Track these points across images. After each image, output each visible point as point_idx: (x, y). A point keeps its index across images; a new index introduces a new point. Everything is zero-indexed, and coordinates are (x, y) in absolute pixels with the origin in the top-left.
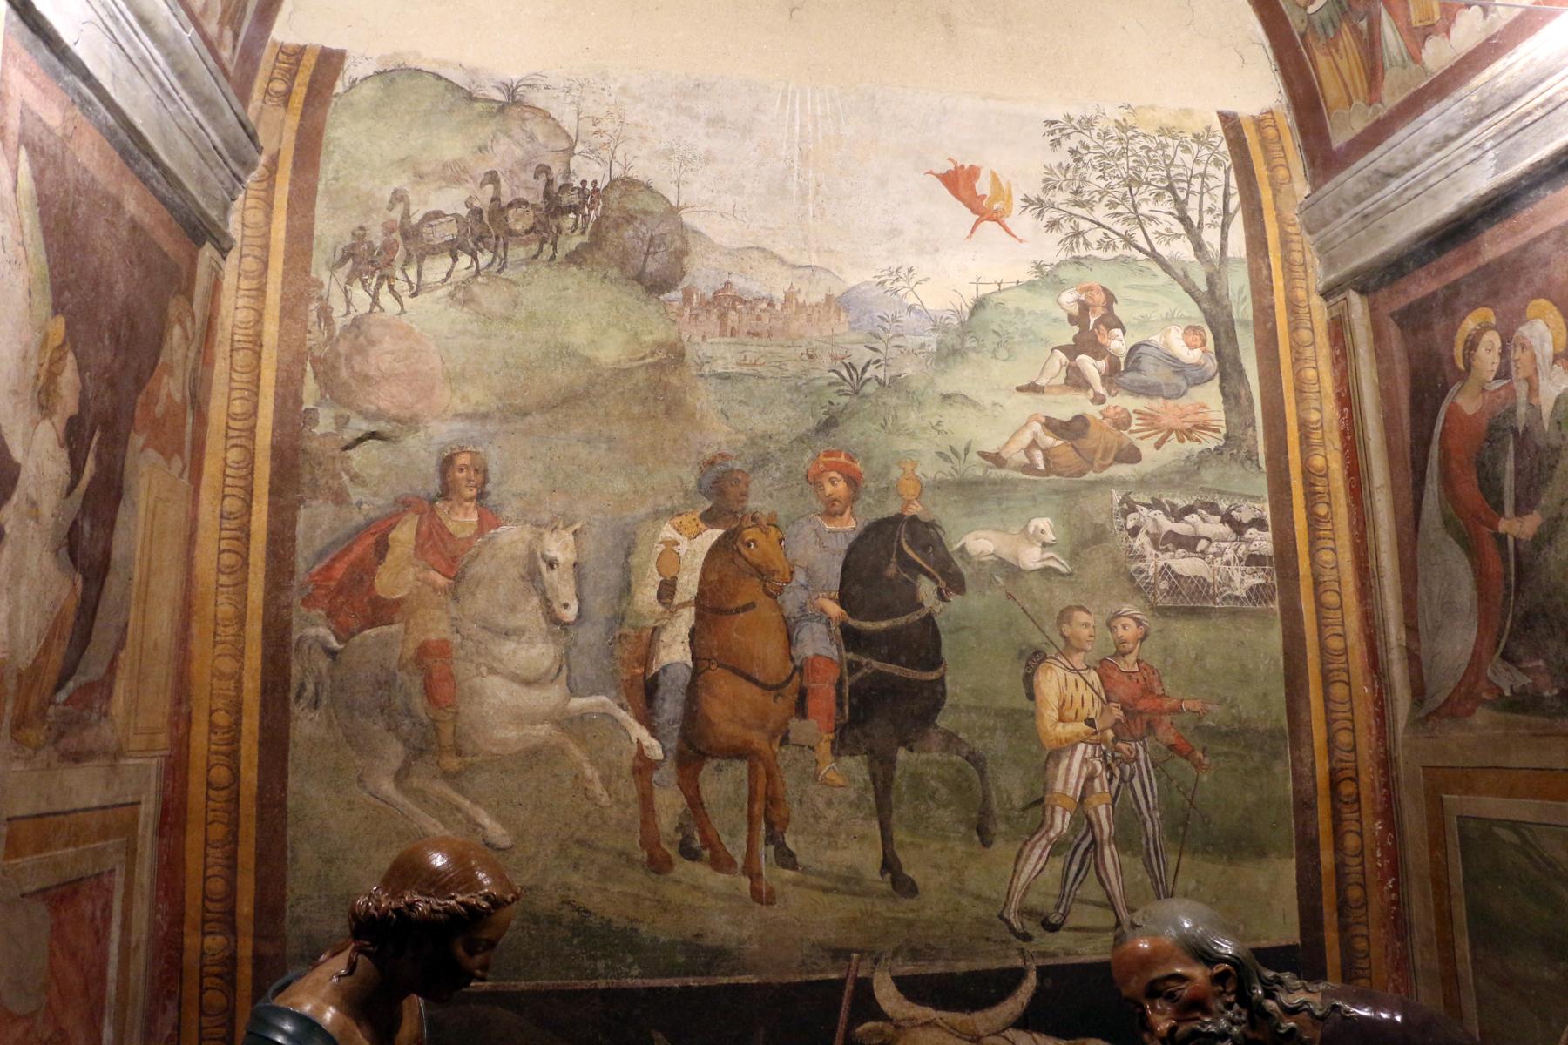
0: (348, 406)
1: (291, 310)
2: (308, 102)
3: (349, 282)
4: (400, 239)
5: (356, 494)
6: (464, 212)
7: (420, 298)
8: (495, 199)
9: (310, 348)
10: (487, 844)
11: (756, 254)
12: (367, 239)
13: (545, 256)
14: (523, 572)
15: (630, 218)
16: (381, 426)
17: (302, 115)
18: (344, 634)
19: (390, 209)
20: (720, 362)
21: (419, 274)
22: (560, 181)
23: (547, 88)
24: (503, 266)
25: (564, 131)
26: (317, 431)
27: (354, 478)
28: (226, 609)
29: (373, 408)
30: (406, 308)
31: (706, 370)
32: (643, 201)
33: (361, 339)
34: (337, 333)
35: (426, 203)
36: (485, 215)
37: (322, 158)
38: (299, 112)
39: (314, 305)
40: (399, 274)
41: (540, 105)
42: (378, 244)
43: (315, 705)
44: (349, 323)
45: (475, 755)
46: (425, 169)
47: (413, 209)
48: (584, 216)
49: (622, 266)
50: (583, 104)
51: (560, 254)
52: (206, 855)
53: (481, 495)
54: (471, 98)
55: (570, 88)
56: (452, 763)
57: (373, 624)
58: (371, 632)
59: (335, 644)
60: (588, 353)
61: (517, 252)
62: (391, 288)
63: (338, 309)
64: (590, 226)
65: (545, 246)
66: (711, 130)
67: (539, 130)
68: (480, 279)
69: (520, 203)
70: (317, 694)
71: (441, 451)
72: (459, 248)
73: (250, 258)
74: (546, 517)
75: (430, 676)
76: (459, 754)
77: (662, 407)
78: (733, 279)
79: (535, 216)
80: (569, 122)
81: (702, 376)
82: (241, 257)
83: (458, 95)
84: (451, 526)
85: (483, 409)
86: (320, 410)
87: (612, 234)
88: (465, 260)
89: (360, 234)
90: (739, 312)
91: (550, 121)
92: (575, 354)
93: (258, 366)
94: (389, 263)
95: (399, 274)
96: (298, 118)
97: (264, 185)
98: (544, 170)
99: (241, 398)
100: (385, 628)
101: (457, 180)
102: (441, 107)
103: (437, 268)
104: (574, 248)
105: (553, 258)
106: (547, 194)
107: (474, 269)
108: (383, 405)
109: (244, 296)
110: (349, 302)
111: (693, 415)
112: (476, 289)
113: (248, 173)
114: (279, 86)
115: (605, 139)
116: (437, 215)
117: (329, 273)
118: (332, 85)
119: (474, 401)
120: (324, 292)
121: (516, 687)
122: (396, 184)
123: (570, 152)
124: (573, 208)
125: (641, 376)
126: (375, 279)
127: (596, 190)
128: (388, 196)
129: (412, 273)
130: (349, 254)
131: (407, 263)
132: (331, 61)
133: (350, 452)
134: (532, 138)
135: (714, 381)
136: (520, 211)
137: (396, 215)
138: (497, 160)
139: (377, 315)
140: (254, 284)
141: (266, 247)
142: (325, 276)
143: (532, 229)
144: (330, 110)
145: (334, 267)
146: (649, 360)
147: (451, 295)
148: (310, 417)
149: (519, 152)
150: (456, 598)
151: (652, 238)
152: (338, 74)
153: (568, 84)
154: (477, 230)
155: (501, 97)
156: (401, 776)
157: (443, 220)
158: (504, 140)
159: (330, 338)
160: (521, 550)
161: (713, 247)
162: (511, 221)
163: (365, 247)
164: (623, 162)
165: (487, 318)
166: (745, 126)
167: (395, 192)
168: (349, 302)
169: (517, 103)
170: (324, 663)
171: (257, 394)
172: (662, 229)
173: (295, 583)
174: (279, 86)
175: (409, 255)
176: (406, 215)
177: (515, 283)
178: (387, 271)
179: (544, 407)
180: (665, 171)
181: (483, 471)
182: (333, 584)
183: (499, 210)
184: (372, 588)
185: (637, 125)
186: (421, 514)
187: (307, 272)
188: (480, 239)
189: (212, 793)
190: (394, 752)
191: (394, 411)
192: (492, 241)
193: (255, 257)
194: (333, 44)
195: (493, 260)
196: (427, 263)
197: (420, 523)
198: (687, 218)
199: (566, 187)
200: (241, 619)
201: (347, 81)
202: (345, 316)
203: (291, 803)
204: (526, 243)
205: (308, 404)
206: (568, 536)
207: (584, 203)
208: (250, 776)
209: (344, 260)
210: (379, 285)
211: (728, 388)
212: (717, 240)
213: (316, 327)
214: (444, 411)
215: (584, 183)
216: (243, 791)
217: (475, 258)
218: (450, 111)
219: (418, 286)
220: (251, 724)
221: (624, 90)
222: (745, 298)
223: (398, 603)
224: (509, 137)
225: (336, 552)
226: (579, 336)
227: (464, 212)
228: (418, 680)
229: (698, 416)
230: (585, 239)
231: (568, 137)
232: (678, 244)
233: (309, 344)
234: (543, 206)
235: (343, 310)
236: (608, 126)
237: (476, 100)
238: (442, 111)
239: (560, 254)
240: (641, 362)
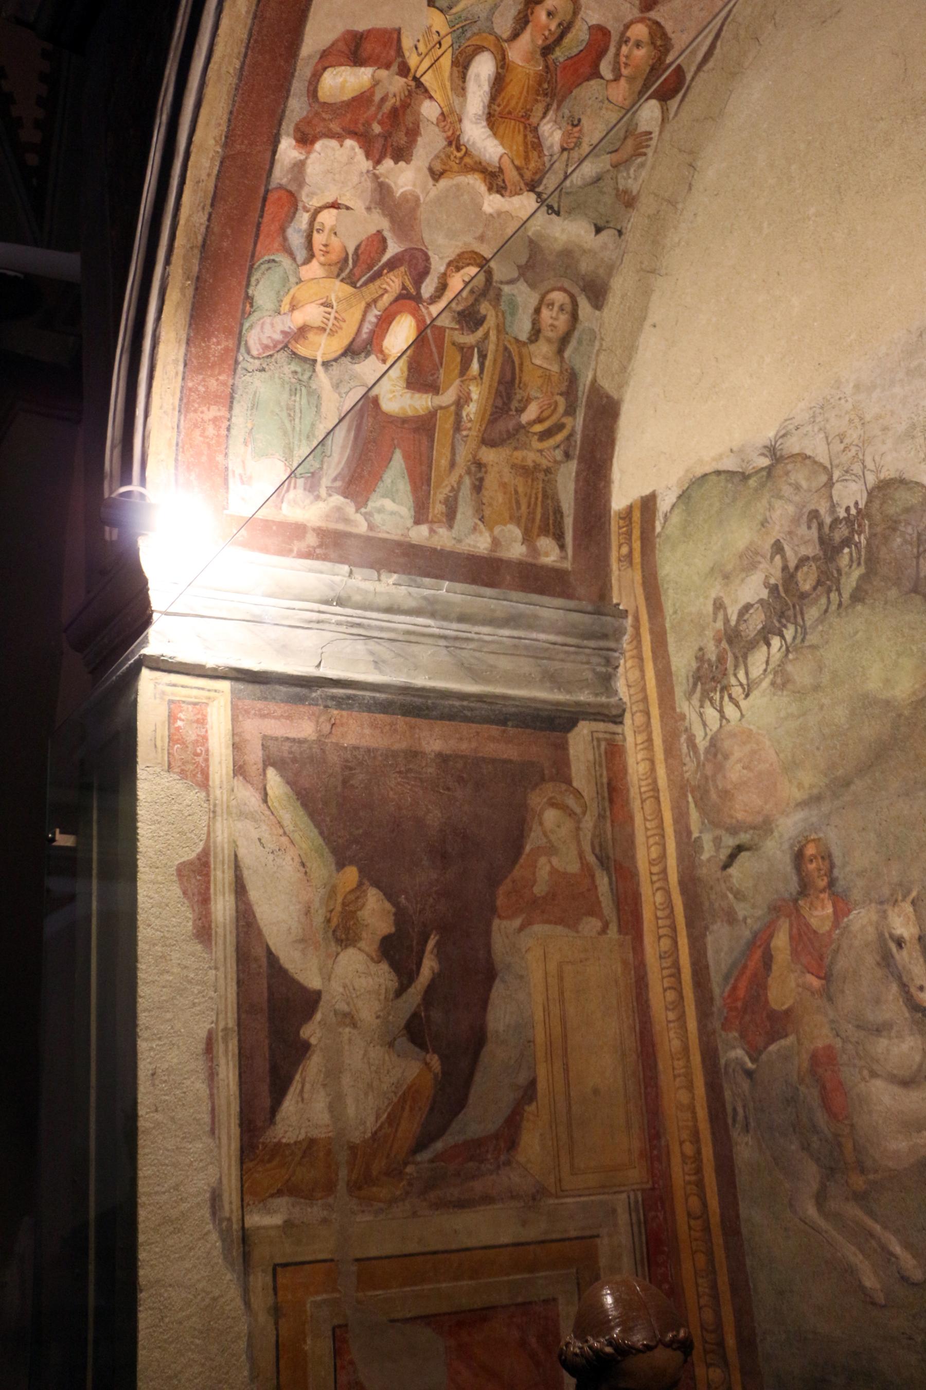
1: (670, 751)
2: (643, 553)
5: (742, 910)
8: (785, 568)
9: (688, 780)
10: (903, 1278)
12: (706, 657)
13: (834, 607)
14: (878, 959)
15: (893, 525)
16: (744, 837)
17: (642, 567)
18: (755, 1053)
19: (715, 621)
21: (747, 674)
22: (828, 520)
23: (797, 429)
24: (805, 633)
26: (705, 857)
27: (739, 896)
28: (676, 1044)
30: (744, 713)
32: (904, 498)
33: (719, 756)
34: (702, 758)
35: (736, 602)
36: (781, 588)
37: (663, 598)
39: (683, 738)
41: (796, 450)
42: (714, 658)
43: (746, 1128)
44: (707, 744)
45: (876, 1171)
46: (729, 567)
48: (856, 546)
49: (897, 583)
50: (828, 426)
51: (846, 595)
52: (697, 1285)
53: (832, 883)
54: (744, 477)
55: (814, 417)
56: (859, 1182)
57: (773, 1040)
58: (773, 1048)
59: (750, 1065)
60: (886, 695)
61: (812, 614)
63: (699, 732)
64: (863, 553)
67: (800, 476)
68: (791, 656)
69: (803, 560)
70: (746, 1118)
71: (791, 847)
72: (769, 633)
73: (638, 714)
74: (886, 891)
75: (824, 1087)
76: (863, 1171)
79: (818, 568)
80: (820, 452)
82: (633, 715)
83: (736, 479)
84: (814, 922)
85: (815, 791)
86: (703, 835)
87: (883, 553)
89: (700, 657)
91: (807, 462)
93: (660, 811)
94: (725, 674)
95: (733, 681)
98: (814, 515)
100: (783, 1042)
101: (752, 566)
102: (727, 500)
103: (758, 661)
104: (854, 584)
105: (840, 605)
106: (822, 540)
107: (784, 648)
108: (740, 816)
109: (642, 749)
110: (705, 725)
113: (618, 640)
116: (747, 607)
117: (687, 703)
118: (654, 528)
119: (807, 786)
120: (687, 723)
121: (896, 1089)
122: (713, 594)
126: (718, 693)
128: (710, 608)
129: (741, 675)
130: (698, 678)
131: (736, 667)
132: (648, 504)
133: (731, 870)
134: (797, 487)
136: (805, 569)
137: (719, 625)
139: (727, 728)
143: (819, 583)
145: (689, 695)
147: (773, 684)
148: (697, 846)
149: (791, 509)
150: (830, 999)
153: (811, 412)
155: (765, 462)
156: (821, 1198)
157: (751, 611)
158: (778, 504)
159: (698, 763)
160: (871, 934)
162: (801, 583)
163: (706, 666)
164: (873, 468)
165: (801, 694)
167: (715, 604)
168: (705, 725)
170: (745, 1085)
171: (663, 837)
173: (715, 1009)
174: (625, 550)
175: (736, 658)
176: (727, 621)
178: (725, 682)
179: (863, 769)
180: (913, 453)
181: (827, 857)
182: (739, 1004)
183: (789, 576)
184: (767, 1002)
185: (878, 417)
186: (789, 916)
187: (674, 709)
188: (782, 615)
189: (692, 1222)
190: (811, 1172)
193: (641, 711)
194: (647, 492)
195: (796, 631)
196: (750, 659)
197: (791, 925)
199: (836, 521)
200: (686, 1049)
201: (661, 518)
202: (704, 739)
203: (744, 1231)
206: (908, 908)
208: (714, 1202)
209: (695, 685)
210: (722, 698)
213: (688, 759)
214: (788, 804)
215: (848, 509)
216: (712, 1221)
217: (783, 637)
218: (734, 500)
219: (748, 685)
220: (708, 1152)
221: (857, 387)
223: (788, 1012)
225: (736, 973)
226: (873, 684)
228: (815, 1092)
230: (862, 570)
231: (825, 468)
234: (821, 554)
235: (702, 733)
236: (853, 436)
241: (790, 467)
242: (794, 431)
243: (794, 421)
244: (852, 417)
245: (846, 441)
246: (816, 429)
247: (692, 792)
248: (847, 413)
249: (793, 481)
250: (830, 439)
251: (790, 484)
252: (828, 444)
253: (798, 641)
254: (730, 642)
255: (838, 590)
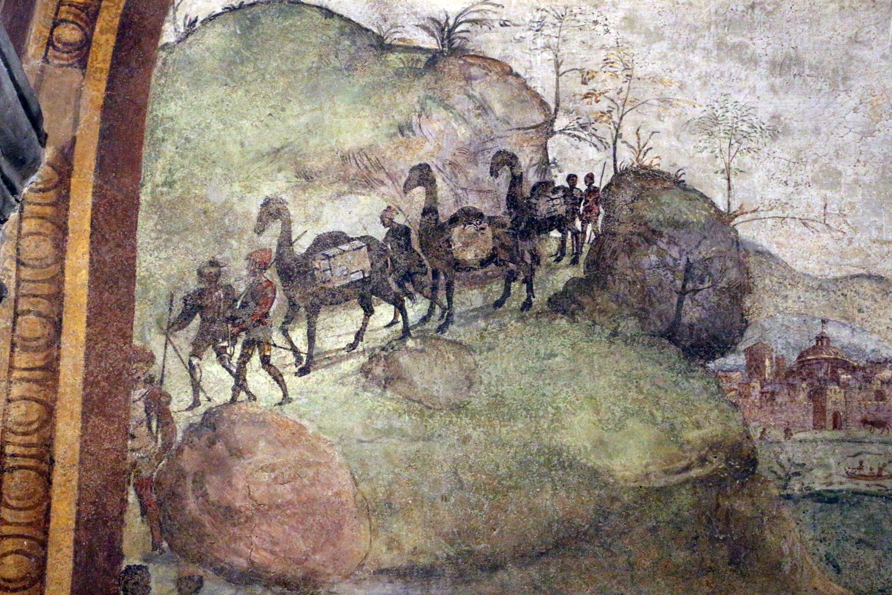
0: (200, 560)
2: (118, 60)
3: (196, 353)
4: (277, 280)
6: (379, 232)
7: (314, 376)
8: (429, 211)
9: (134, 465)
11: (867, 287)
12: (223, 281)
13: (514, 303)
15: (650, 235)
17: (111, 80)
19: (259, 231)
20: (819, 473)
21: (311, 338)
22: (532, 178)
23: (503, 25)
24: (448, 320)
25: (536, 95)
29: (241, 563)
30: (290, 394)
31: (795, 487)
33: (220, 446)
34: (179, 437)
35: (317, 220)
36: (414, 236)
37: (146, 151)
38: (104, 76)
40: (277, 338)
44: (198, 419)
46: (315, 164)
47: (296, 230)
48: (575, 234)
49: (642, 315)
50: (564, 49)
51: (540, 298)
55: (541, 23)
60: (595, 461)
62: (265, 361)
64: (586, 249)
65: (515, 286)
66: (778, 81)
68: (410, 343)
72: (372, 292)
73: (31, 317)
77: (724, 552)
78: (831, 331)
79: (495, 237)
81: (789, 497)
82: (16, 315)
85: (423, 561)
86: (151, 567)
87: (623, 263)
88: (384, 312)
90: (845, 386)
91: (511, 79)
92: (570, 465)
93: (47, 497)
94: (262, 320)
95: (277, 338)
96: (103, 85)
97: (52, 195)
98: (507, 160)
99: (17, 552)
101: (367, 182)
102: (336, 63)
104: (561, 286)
105: (527, 305)
106: (512, 200)
107: (400, 326)
108: (261, 557)
109: (22, 379)
110: (196, 387)
111: (778, 566)
112: (404, 360)
113: (25, 178)
114: (70, 34)
115: (604, 105)
116: (337, 239)
117: (163, 339)
118: (156, 32)
119: (408, 548)
120: (155, 370)
122: (267, 190)
123: (547, 129)
124: (559, 223)
125: (685, 499)
126: (239, 347)
127: (592, 191)
128: (255, 210)
129: (299, 336)
131: (289, 319)
134: (484, 108)
135: (811, 506)
136: (471, 229)
137: (270, 239)
138: (428, 147)
139: (245, 407)
140: (38, 359)
141: (57, 297)
142: (156, 343)
143: (492, 258)
144: (155, 71)
145: (172, 327)
146: (695, 473)
147: (365, 371)
149: (463, 132)
151: (689, 267)
152: (166, 13)
153: (538, 16)
154: (402, 262)
155: (431, 43)
157: (345, 247)
158: (439, 113)
159: (166, 446)
161: (792, 278)
162: (457, 245)
163: (220, 293)
164: (634, 143)
166: (835, 71)
167: (267, 203)
168: (196, 387)
169: (459, 52)
171: (44, 545)
172: (705, 250)
174: (70, 34)
175: (293, 305)
176: (286, 241)
177: (469, 349)
178: (258, 333)
180: (705, 154)
185: (655, 80)
187: (127, 337)
188: (408, 276)
191: (277, 568)
192: (428, 279)
193: (39, 314)
195: (431, 311)
196: (323, 319)
198: (745, 231)
199: (544, 187)
201: (180, 23)
202: (190, 408)
204: (482, 282)
205: (132, 559)
207: (574, 212)
210: (245, 358)
211: (835, 517)
212: (798, 266)
213: (144, 429)
214: (361, 566)
215: (572, 178)
217: (401, 309)
219: (310, 356)
221: (630, 22)
222: (854, 361)
224: (447, 107)
227: (379, 232)
229: (787, 568)
230: (579, 272)
231: (543, 104)
232: (733, 274)
233: (132, 457)
234: (507, 220)
235: (188, 399)
236: (606, 83)
237: (391, 48)
238: (335, 69)
239: (540, 298)
240: (684, 476)
241: (474, 71)
242: (497, 24)
243: (504, 11)
244: (612, 58)
245: (592, 85)
246: (540, 42)
247: (140, 488)
248: (603, 47)
249: (476, 94)
250: (562, 69)
251: (470, 97)
252: (558, 75)
253: (434, 324)
254: (286, 274)
255: (528, 282)
